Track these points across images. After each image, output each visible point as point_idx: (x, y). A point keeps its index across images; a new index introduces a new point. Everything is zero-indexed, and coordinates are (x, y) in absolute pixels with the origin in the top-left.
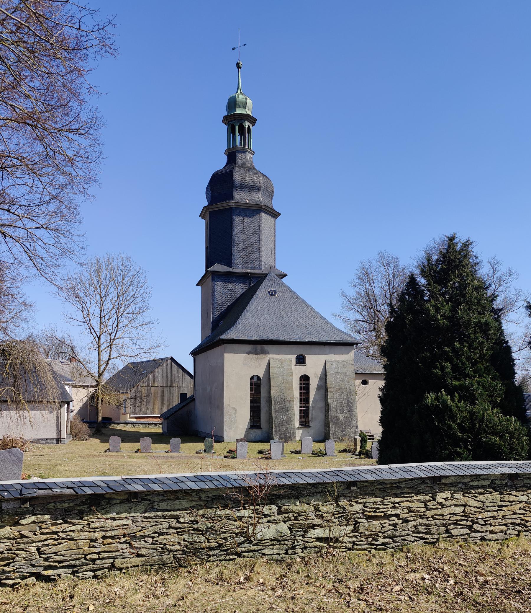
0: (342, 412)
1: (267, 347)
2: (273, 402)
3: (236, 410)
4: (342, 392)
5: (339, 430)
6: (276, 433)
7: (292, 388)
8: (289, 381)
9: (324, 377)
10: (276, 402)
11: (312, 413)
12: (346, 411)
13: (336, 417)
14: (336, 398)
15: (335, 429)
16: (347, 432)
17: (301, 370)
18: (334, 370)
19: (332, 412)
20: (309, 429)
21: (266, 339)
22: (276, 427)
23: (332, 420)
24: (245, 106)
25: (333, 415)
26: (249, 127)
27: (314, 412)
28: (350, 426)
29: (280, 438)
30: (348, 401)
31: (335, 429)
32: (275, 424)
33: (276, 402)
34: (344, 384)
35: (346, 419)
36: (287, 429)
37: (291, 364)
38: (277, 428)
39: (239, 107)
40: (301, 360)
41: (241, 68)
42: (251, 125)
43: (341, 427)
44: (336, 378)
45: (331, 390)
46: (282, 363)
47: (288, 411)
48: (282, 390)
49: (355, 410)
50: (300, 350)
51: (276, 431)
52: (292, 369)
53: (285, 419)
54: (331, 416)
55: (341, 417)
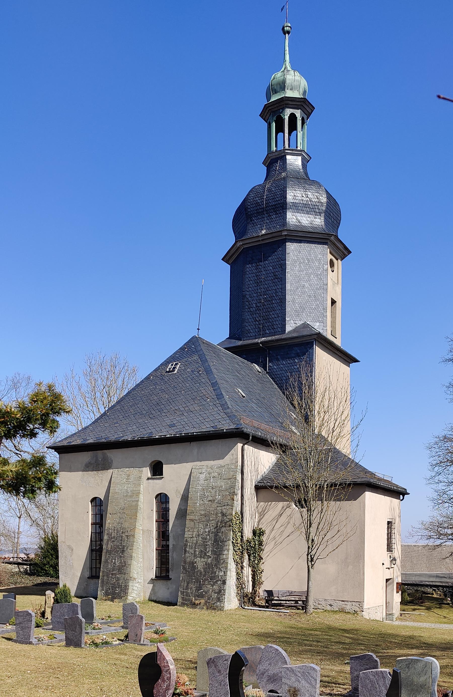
0: (203, 554)
1: (112, 454)
2: (106, 537)
3: (72, 550)
4: (209, 520)
5: (193, 586)
6: (102, 586)
7: (134, 516)
8: (134, 504)
9: (185, 498)
10: (110, 537)
11: (173, 556)
12: (209, 554)
13: (192, 564)
14: (198, 532)
15: (188, 583)
16: (206, 589)
17: (159, 486)
18: (202, 482)
19: (187, 555)
20: (169, 582)
21: (103, 440)
22: (103, 576)
23: (184, 568)
24: (282, 86)
25: (188, 560)
26: (293, 117)
27: (175, 556)
28: (214, 579)
29: (107, 594)
30: (216, 535)
31: (188, 583)
32: (103, 572)
33: (110, 537)
34: (215, 505)
35: (208, 566)
36: (118, 579)
37: (140, 477)
38: (105, 578)
39: (276, 92)
40: (157, 470)
41: (288, 32)
42: (298, 113)
43: (198, 581)
44: (203, 497)
45: (192, 517)
46: (129, 476)
47: (123, 551)
48: (120, 518)
49: (225, 552)
50: (153, 453)
51: (103, 582)
52: (139, 485)
53: (117, 564)
54: (185, 562)
55: (200, 563)
